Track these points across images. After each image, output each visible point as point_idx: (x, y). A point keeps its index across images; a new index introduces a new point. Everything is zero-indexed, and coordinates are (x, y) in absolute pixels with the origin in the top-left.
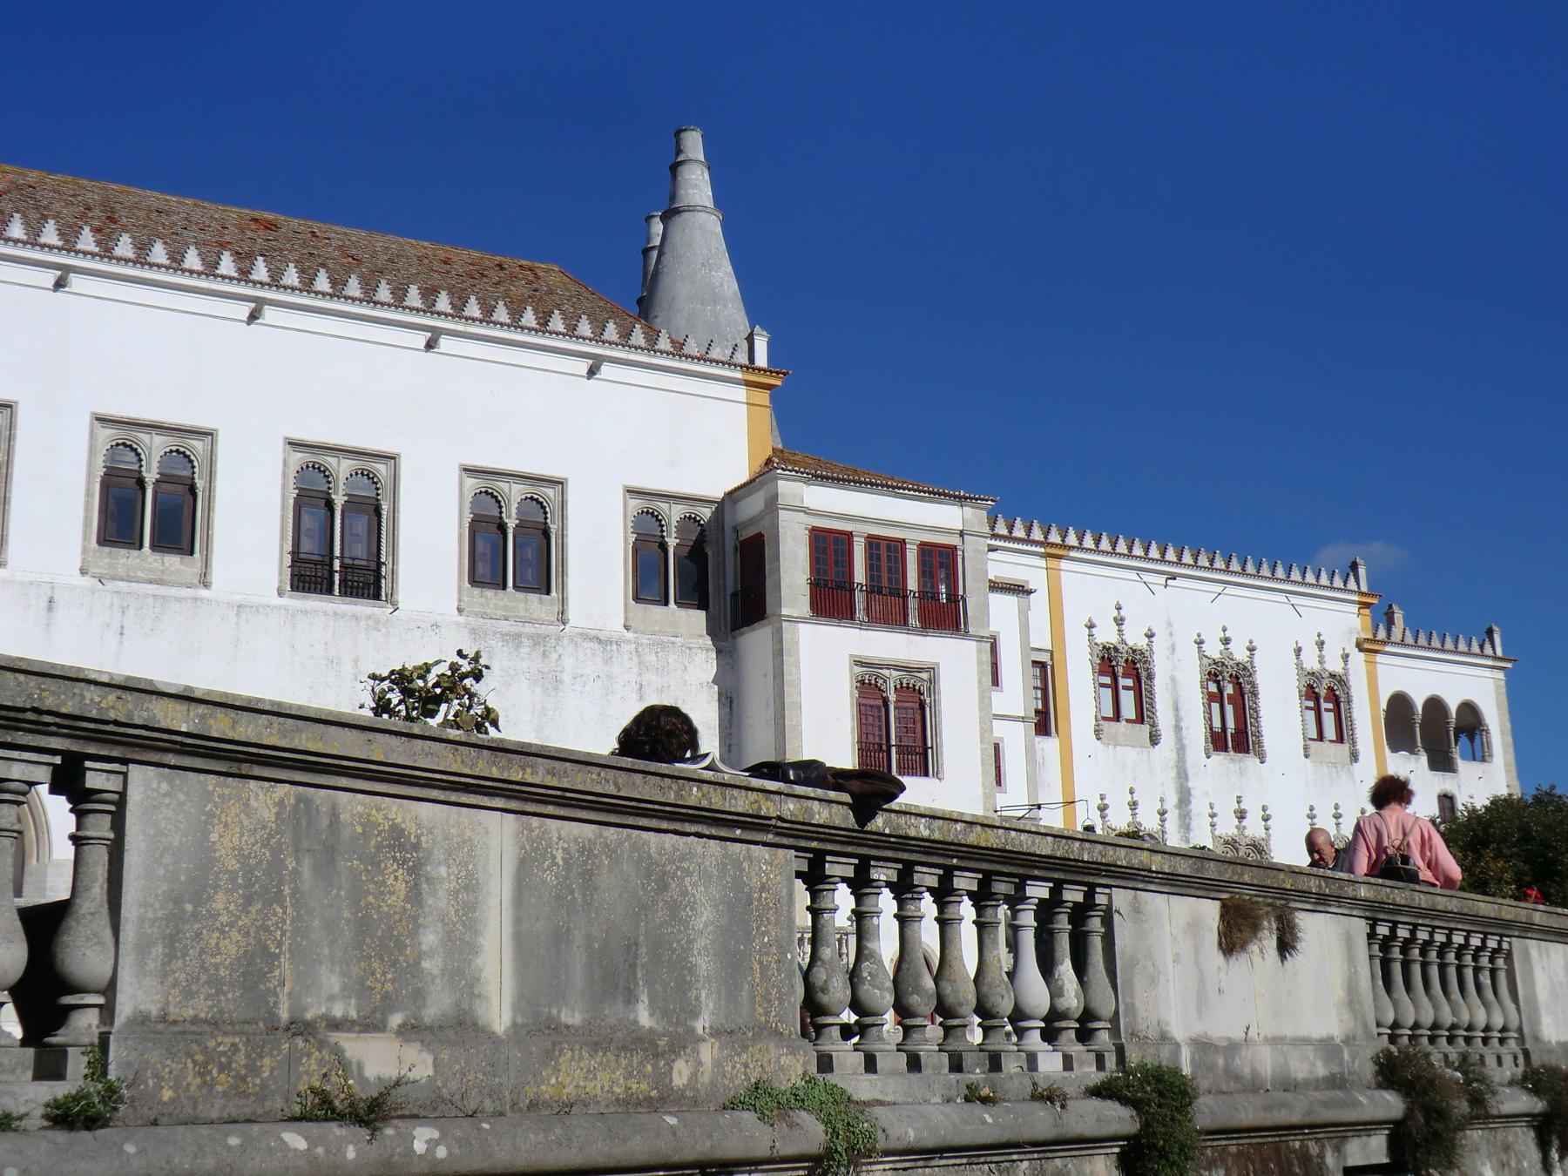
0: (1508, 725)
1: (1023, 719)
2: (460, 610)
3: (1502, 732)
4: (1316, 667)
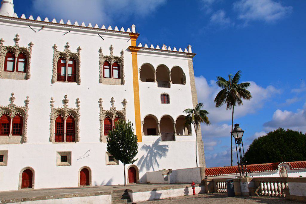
0: (193, 74)
3: (191, 75)
4: (108, 55)
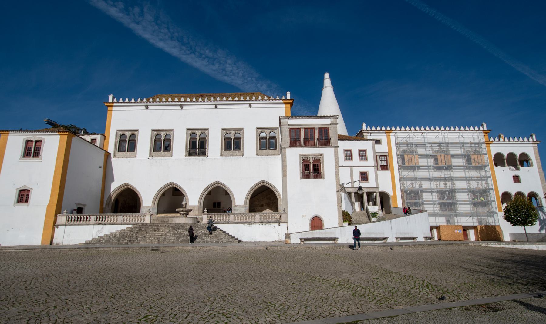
1: (373, 167)
2: (221, 156)
